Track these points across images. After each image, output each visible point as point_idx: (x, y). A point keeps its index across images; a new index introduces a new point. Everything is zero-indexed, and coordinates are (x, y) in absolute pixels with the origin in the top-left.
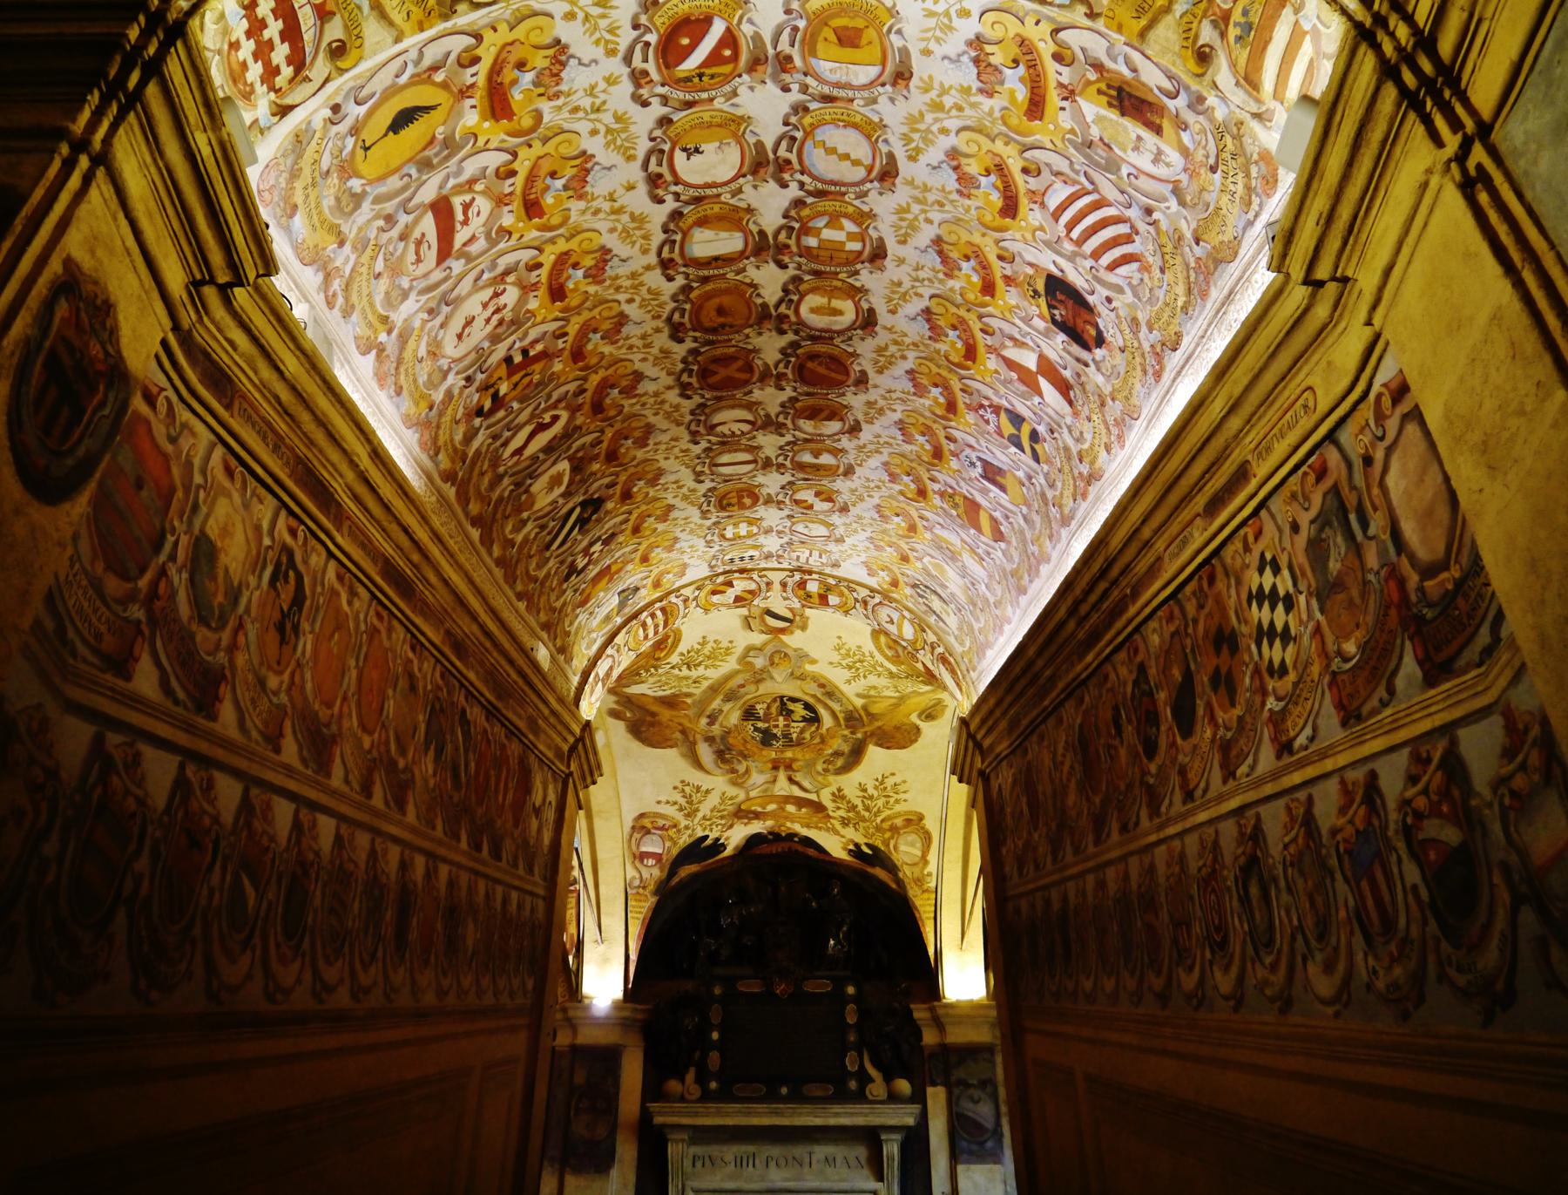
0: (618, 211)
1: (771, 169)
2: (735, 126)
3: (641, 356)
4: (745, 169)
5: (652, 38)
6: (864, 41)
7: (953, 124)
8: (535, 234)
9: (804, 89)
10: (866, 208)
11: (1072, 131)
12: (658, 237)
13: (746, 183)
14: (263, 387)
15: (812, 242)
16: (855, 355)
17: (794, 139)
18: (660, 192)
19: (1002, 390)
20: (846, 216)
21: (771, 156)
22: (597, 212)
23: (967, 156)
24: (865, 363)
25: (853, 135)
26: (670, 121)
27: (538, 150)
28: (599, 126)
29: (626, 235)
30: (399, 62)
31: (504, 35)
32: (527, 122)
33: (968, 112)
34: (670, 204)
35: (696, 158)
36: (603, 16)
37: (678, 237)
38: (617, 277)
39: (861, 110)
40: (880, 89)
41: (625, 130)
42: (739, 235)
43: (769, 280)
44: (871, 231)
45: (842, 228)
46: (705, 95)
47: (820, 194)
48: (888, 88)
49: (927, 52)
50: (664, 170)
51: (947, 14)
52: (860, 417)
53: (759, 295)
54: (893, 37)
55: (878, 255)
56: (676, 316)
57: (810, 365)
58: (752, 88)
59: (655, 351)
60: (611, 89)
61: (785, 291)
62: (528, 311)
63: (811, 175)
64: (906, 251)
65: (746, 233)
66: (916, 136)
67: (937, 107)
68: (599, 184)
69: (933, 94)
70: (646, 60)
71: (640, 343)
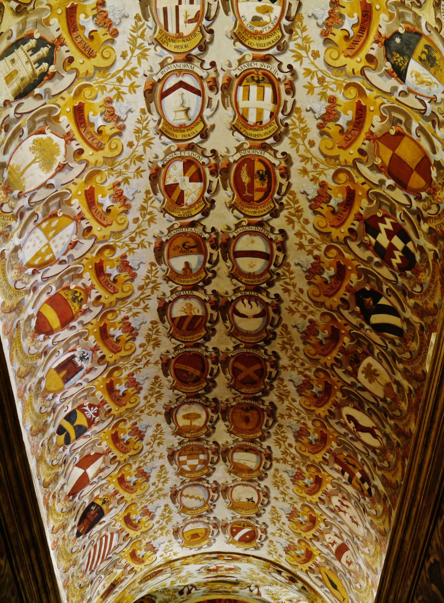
0: (282, 493)
1: (220, 489)
3: (294, 404)
4: (231, 489)
5: (258, 541)
7: (156, 526)
8: (316, 511)
9: (209, 518)
10: (181, 477)
11: (120, 562)
12: (271, 473)
13: (230, 483)
15: (202, 457)
16: (173, 388)
17: (212, 500)
18: (265, 490)
19: (94, 438)
20: (188, 472)
21: (220, 494)
22: (291, 499)
24: (167, 382)
25: (189, 505)
26: (257, 515)
27: (304, 534)
29: (283, 482)
31: (300, 566)
33: (152, 533)
34: (263, 484)
35: (250, 497)
37: (261, 469)
38: (293, 466)
41: (273, 518)
42: (235, 461)
43: (222, 435)
44: (177, 467)
45: (189, 466)
46: (243, 520)
49: (170, 541)
50: (262, 498)
51: (166, 553)
52: (160, 326)
53: (227, 427)
55: (171, 457)
56: (271, 422)
57: (198, 373)
59: (286, 403)
61: (214, 428)
62: (333, 487)
63: (204, 487)
64: (158, 463)
65: (231, 461)
66: (167, 515)
68: (287, 506)
69: (165, 531)
70: (261, 536)
71: (293, 413)
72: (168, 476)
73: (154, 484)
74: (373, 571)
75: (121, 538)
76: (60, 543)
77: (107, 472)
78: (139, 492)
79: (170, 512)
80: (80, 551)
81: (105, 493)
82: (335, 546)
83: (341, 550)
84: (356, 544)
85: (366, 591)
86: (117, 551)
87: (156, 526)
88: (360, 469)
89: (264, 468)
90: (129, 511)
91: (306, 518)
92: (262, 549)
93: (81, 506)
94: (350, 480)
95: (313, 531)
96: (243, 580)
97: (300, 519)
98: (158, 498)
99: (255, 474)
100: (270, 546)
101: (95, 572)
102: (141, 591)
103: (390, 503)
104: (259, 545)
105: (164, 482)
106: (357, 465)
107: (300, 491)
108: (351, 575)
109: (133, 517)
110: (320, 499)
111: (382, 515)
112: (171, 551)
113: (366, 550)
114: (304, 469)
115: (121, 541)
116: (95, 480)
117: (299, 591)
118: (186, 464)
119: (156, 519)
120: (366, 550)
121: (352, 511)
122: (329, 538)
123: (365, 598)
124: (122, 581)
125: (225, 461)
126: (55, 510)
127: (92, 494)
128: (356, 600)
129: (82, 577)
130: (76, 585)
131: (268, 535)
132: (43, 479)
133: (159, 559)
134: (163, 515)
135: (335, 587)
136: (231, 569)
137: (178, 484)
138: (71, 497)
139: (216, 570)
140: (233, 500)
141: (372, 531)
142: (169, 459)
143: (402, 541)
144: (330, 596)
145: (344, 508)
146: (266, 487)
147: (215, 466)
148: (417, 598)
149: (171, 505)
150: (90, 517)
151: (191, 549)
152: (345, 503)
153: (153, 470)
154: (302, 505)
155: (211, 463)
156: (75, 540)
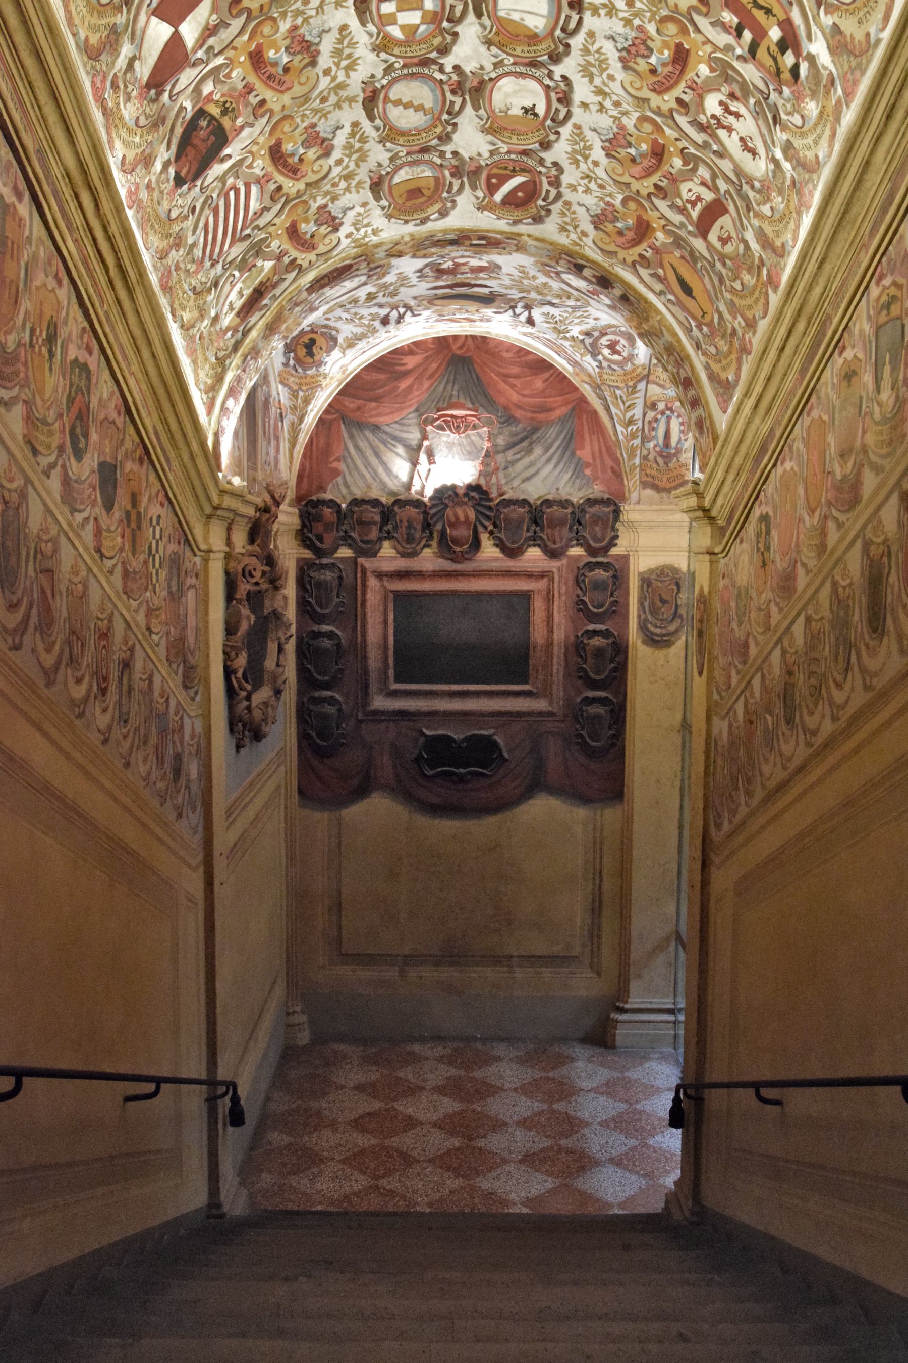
0: (599, 92)
1: (468, 85)
2: (494, 127)
4: (490, 85)
5: (540, 203)
6: (405, 195)
7: (336, 171)
8: (668, 131)
10: (383, 55)
11: (268, 246)
14: (733, 489)
17: (449, 113)
20: (399, 43)
21: (467, 97)
22: (617, 104)
23: (318, 158)
26: (541, 145)
28: (591, 166)
29: (603, 64)
30: (669, 306)
31: (622, 254)
32: (632, 205)
33: (328, 187)
34: (558, 70)
35: (528, 103)
36: (566, 223)
37: (558, 32)
38: (628, 22)
39: (400, 148)
40: (389, 169)
41: (574, 151)
42: (501, 14)
45: (403, 28)
46: (513, 156)
47: (425, 62)
48: (384, 173)
49: (364, 205)
50: (555, 104)
51: (358, 230)
54: (386, 204)
58: (479, 155)
60: (575, 183)
62: (712, 70)
66: (357, 145)
67: (348, 177)
68: (605, 122)
70: (548, 192)
72: (358, 53)
73: (327, 72)
74: (774, 250)
75: (267, 196)
76: (144, 195)
77: (226, 35)
78: (297, 90)
79: (363, 140)
80: (186, 217)
81: (226, 88)
82: (699, 207)
83: (714, 211)
84: (745, 198)
85: (752, 294)
86: (262, 222)
87: (336, 171)
88: (782, 17)
89: (563, 30)
90: (278, 134)
91: (644, 147)
92: (547, 220)
93: (177, 116)
94: (753, 49)
95: (655, 178)
96: (504, 291)
97: (632, 151)
98: (338, 106)
99: (543, 46)
100: (563, 214)
101: (219, 267)
102: (312, 310)
103: (840, 91)
104: (543, 213)
105: (349, 68)
106: (777, 9)
107: (638, 84)
108: (724, 264)
109: (288, 147)
110: (679, 101)
111: (816, 125)
112: (367, 225)
113: (766, 209)
114: (651, 28)
115: (267, 202)
116: (200, 54)
117: (612, 307)
118: (395, 23)
119: (336, 154)
120: (766, 209)
121: (747, 126)
122: (689, 189)
123: (750, 307)
124: (275, 286)
125: (479, 15)
126: (121, 118)
127: (197, 90)
128: (730, 313)
129: (196, 272)
130: (186, 287)
131: (562, 190)
132: (82, 36)
133: (345, 242)
134: (348, 147)
135: (687, 290)
136: (481, 269)
137: (379, 73)
138: (153, 92)
139: (452, 271)
140: (493, 111)
141: (787, 166)
142: (357, 9)
143: (867, 164)
144: (675, 309)
145: (731, 119)
146: (564, 78)
147: (458, 29)
148: (878, 283)
149: (366, 124)
150: (200, 143)
151: (406, 222)
152: (734, 106)
153: (324, 35)
154: (638, 119)
155: (449, 20)
156: (172, 193)
